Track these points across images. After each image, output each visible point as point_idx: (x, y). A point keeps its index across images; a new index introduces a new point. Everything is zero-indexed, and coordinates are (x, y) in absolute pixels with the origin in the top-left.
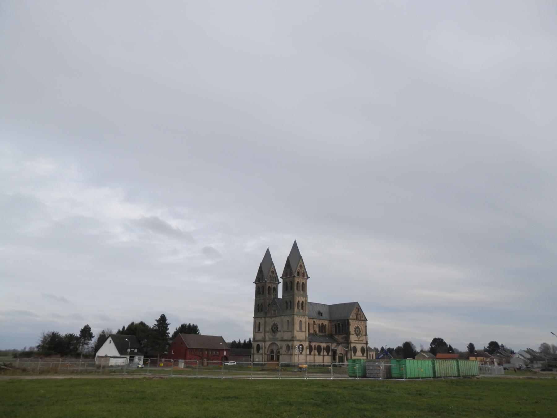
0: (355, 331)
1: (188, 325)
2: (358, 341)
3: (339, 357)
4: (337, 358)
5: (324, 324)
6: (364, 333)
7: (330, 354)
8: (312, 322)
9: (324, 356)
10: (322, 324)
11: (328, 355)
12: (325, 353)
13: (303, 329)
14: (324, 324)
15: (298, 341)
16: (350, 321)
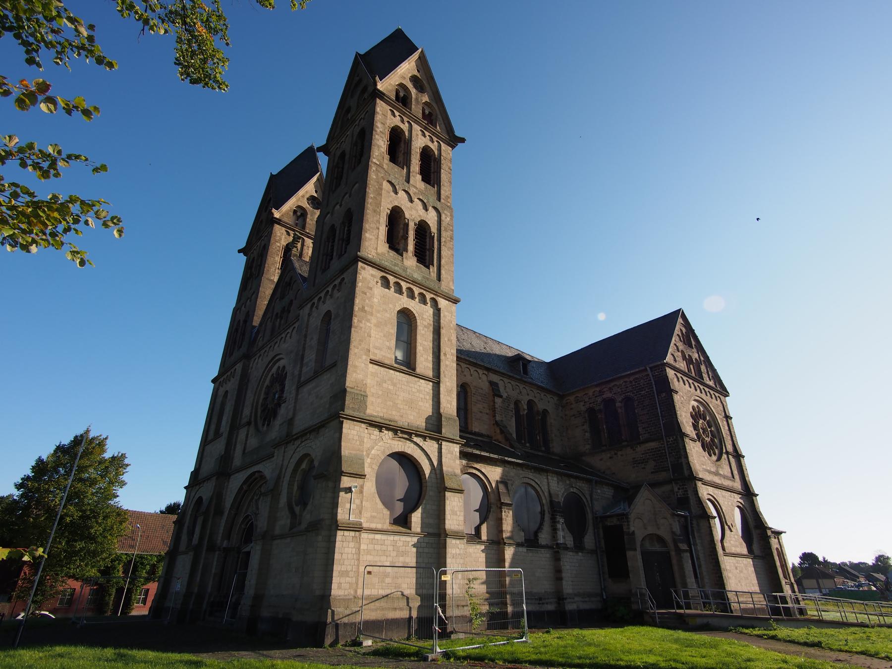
0: (695, 427)
1: (124, 478)
2: (716, 474)
3: (645, 555)
4: (635, 560)
5: (541, 406)
6: (730, 448)
7: (589, 540)
8: (484, 385)
9: (556, 550)
10: (530, 403)
11: (579, 547)
12: (564, 536)
13: (424, 363)
14: (541, 406)
15: (379, 426)
16: (670, 373)
